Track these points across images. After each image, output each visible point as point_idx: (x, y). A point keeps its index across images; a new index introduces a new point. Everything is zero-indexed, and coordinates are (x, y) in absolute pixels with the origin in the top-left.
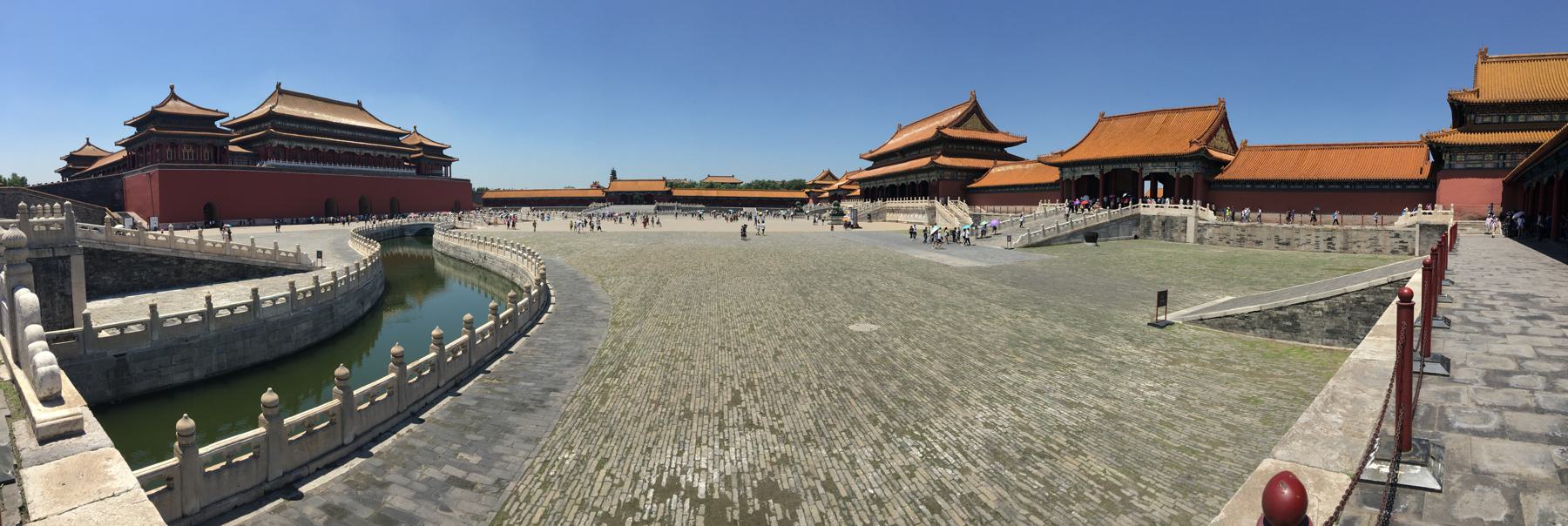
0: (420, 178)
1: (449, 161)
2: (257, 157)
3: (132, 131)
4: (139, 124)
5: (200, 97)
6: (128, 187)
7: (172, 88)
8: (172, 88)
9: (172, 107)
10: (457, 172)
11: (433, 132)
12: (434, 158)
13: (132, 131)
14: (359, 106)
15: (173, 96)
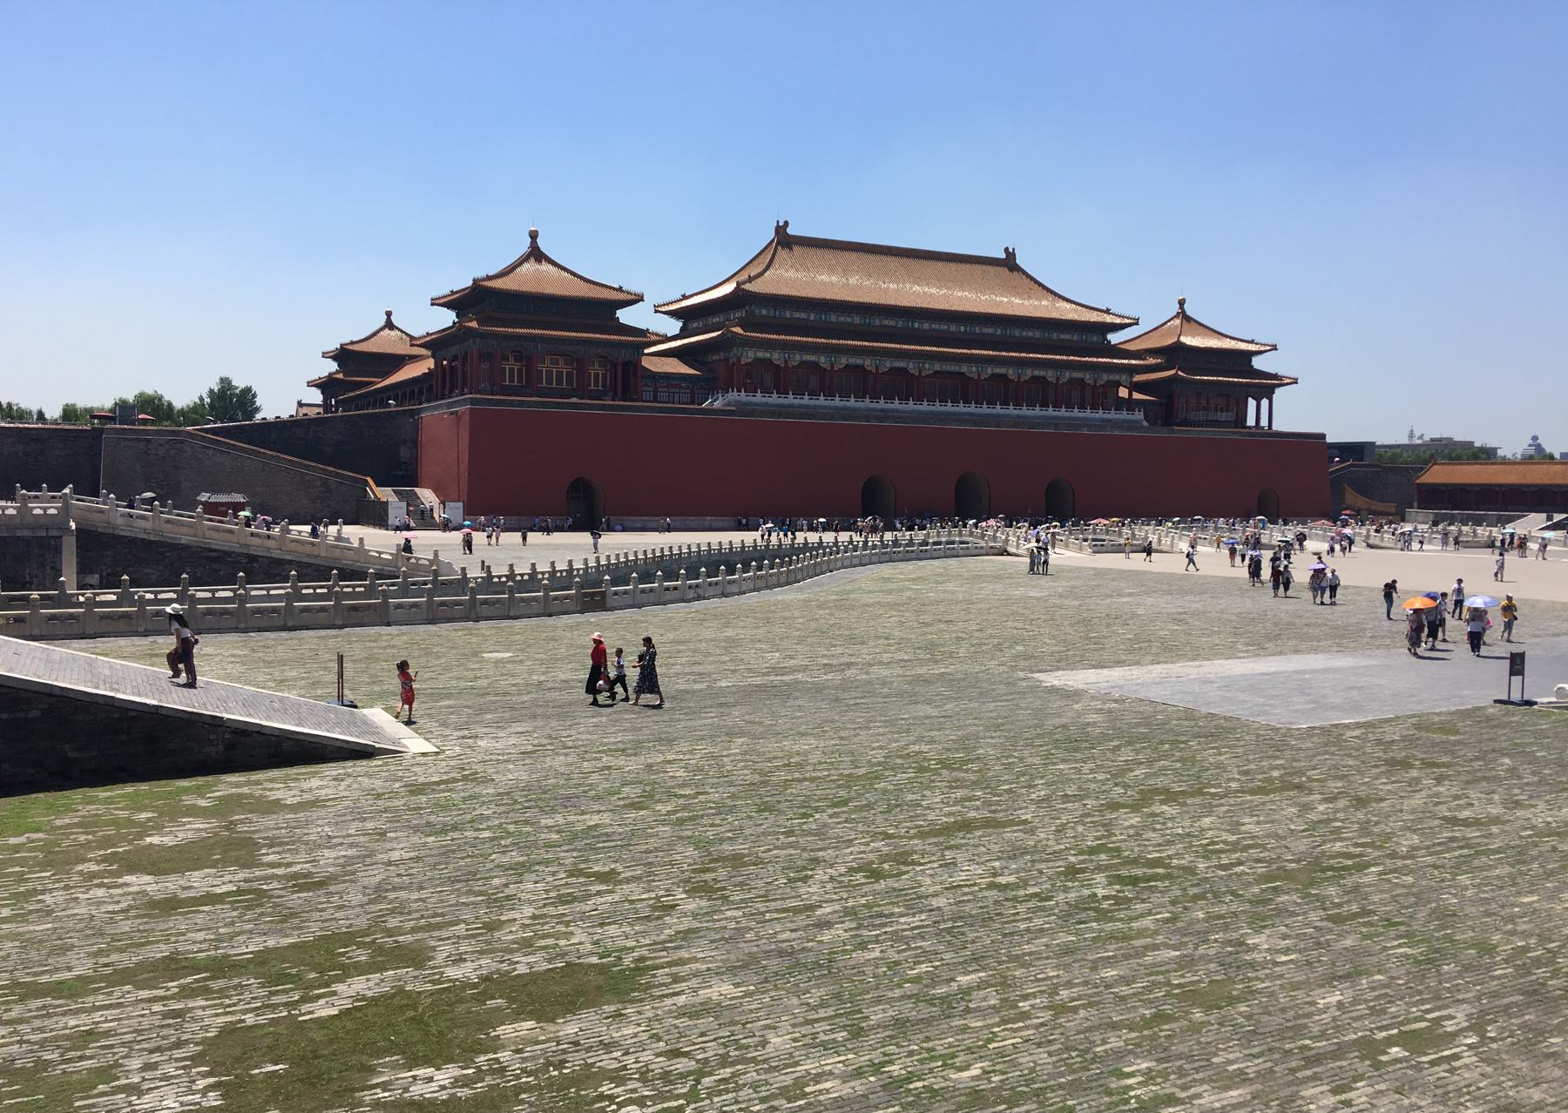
0: (1161, 433)
1: (1266, 386)
2: (709, 384)
3: (447, 318)
4: (460, 302)
5: (591, 256)
6: (425, 436)
7: (534, 236)
8: (534, 236)
9: (532, 278)
10: (1289, 413)
11: (1228, 320)
12: (1234, 376)
13: (447, 318)
14: (1009, 262)
15: (536, 254)
